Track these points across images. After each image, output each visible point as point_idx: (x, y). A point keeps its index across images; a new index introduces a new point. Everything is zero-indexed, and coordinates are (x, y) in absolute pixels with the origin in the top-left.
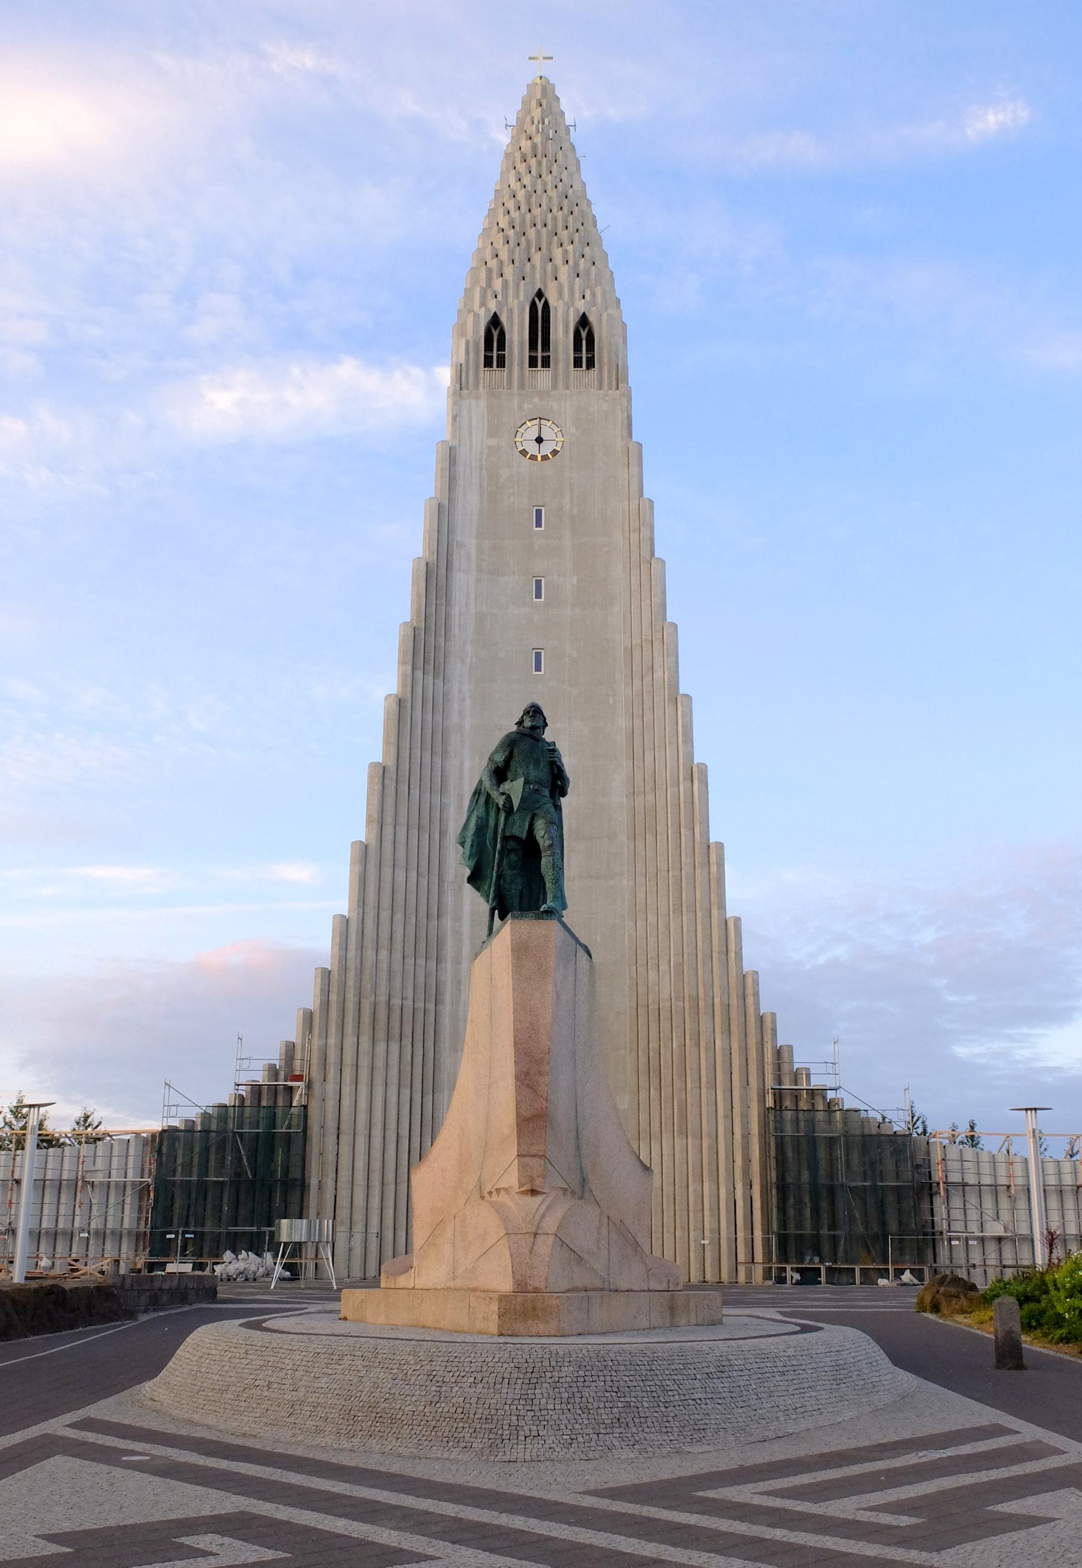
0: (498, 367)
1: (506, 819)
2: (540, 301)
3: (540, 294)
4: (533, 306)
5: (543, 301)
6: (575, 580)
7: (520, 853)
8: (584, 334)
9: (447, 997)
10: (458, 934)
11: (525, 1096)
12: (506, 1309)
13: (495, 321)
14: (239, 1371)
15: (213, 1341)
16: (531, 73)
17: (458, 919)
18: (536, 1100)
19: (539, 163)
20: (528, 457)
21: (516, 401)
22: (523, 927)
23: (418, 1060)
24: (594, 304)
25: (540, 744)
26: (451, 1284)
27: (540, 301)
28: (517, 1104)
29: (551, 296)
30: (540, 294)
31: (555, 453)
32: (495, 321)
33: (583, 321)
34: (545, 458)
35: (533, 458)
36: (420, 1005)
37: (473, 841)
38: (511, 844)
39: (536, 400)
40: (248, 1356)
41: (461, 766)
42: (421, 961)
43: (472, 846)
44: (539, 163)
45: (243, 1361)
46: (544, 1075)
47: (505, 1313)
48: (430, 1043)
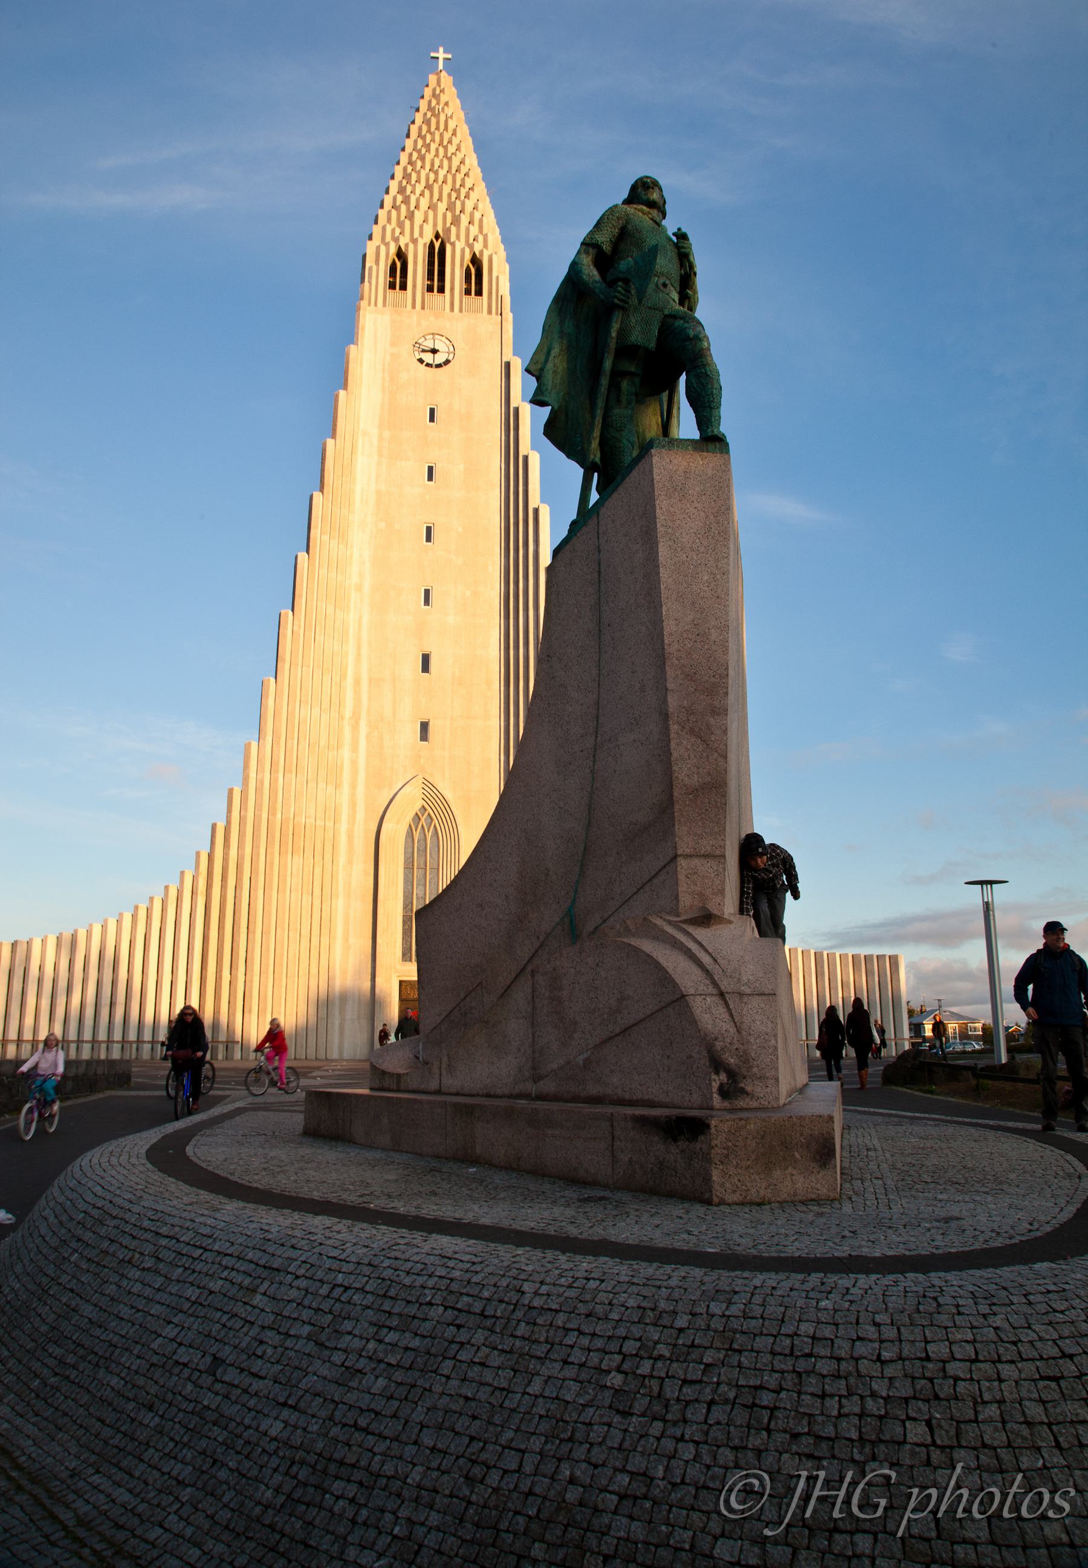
6: (462, 467)
7: (637, 380)
9: (344, 818)
10: (354, 763)
11: (687, 749)
12: (728, 1148)
13: (401, 255)
14: (141, 1303)
15: (90, 1209)
17: (355, 749)
18: (708, 757)
19: (442, 135)
21: (415, 318)
22: (675, 461)
23: (318, 870)
24: (486, 246)
26: (532, 1088)
30: (437, 236)
31: (447, 362)
32: (401, 255)
33: (476, 261)
34: (439, 366)
35: (428, 365)
36: (320, 823)
39: (432, 318)
40: (161, 1266)
41: (360, 619)
42: (322, 785)
44: (442, 135)
45: (149, 1277)
46: (718, 714)
47: (727, 1156)
48: (328, 856)
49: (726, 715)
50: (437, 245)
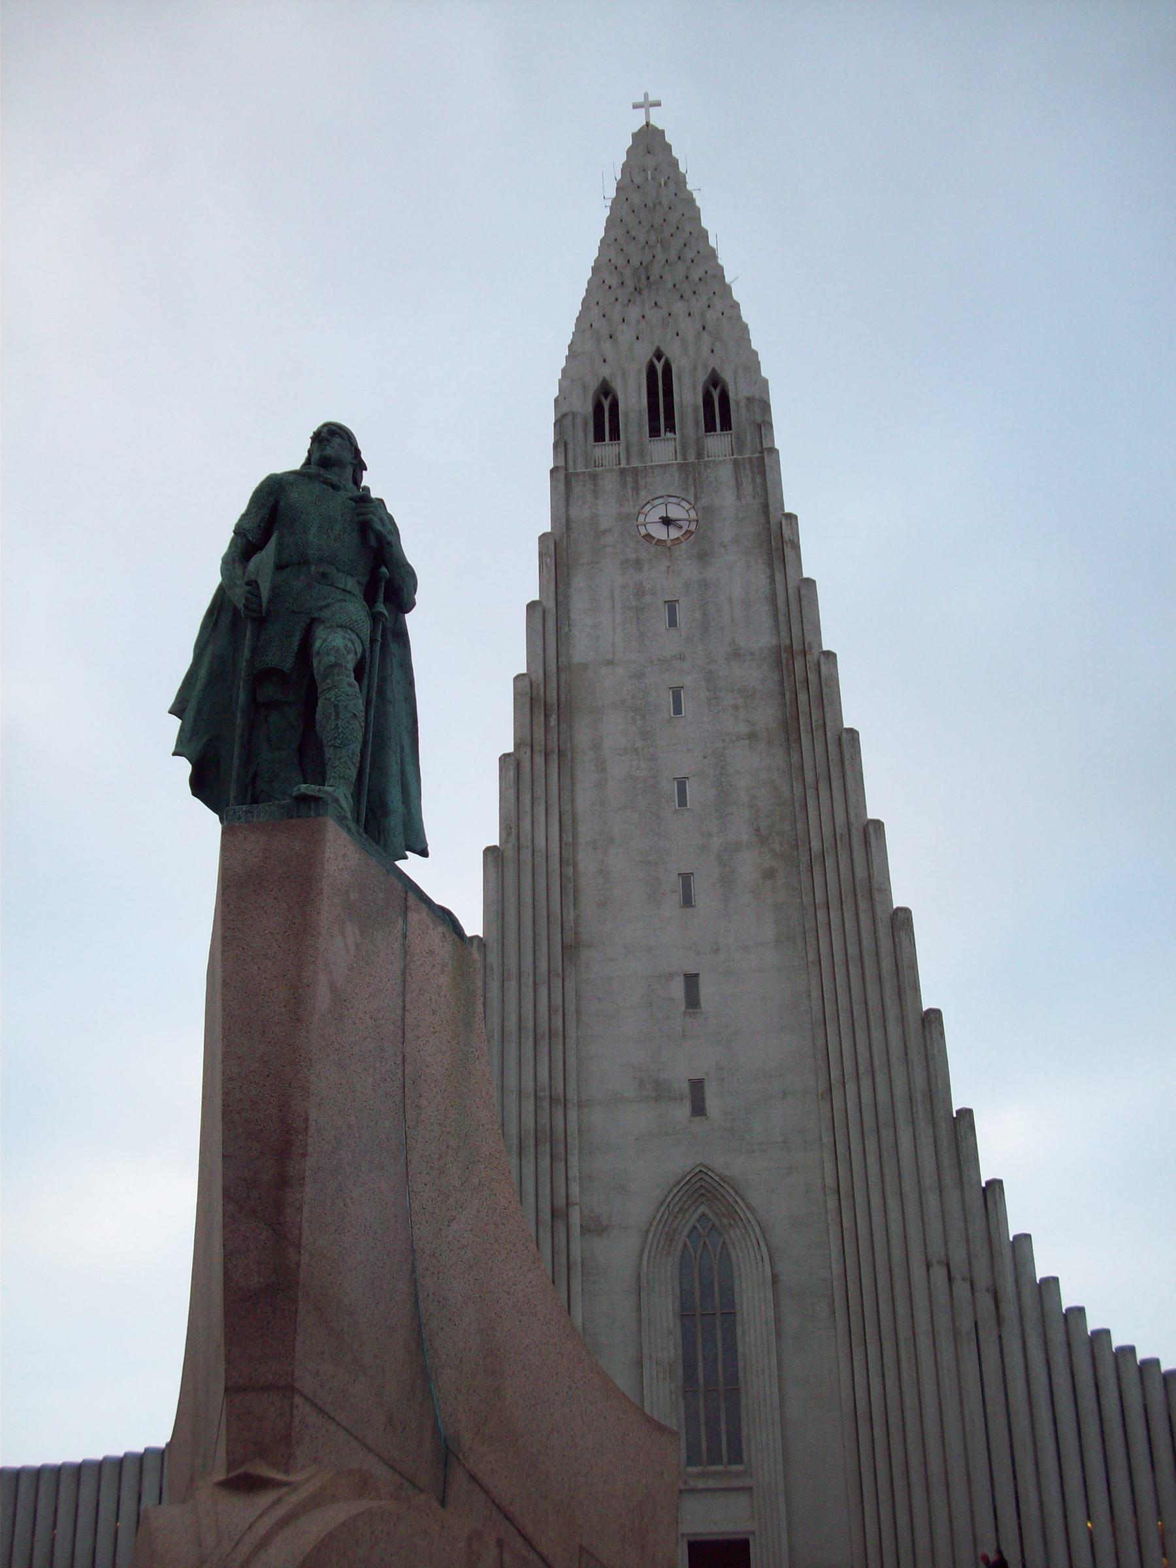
0: (611, 440)
1: (257, 636)
2: (659, 362)
3: (659, 355)
4: (651, 371)
5: (663, 360)
8: (716, 395)
13: (605, 390)
16: (637, 121)
20: (654, 542)
25: (342, 493)
27: (659, 362)
28: (227, 1256)
29: (673, 352)
30: (659, 355)
32: (605, 390)
33: (715, 380)
35: (660, 542)
37: (200, 703)
38: (269, 691)
43: (199, 712)
49: (302, 1185)
50: (659, 367)
